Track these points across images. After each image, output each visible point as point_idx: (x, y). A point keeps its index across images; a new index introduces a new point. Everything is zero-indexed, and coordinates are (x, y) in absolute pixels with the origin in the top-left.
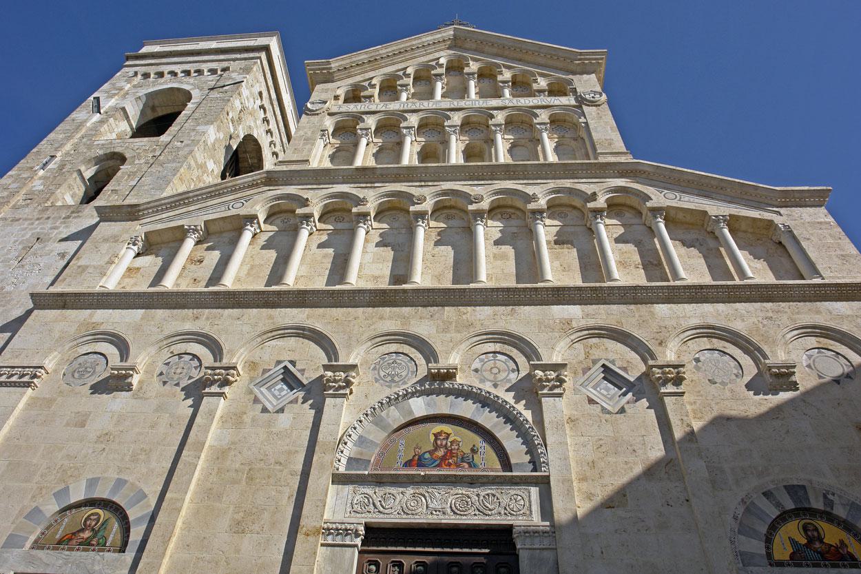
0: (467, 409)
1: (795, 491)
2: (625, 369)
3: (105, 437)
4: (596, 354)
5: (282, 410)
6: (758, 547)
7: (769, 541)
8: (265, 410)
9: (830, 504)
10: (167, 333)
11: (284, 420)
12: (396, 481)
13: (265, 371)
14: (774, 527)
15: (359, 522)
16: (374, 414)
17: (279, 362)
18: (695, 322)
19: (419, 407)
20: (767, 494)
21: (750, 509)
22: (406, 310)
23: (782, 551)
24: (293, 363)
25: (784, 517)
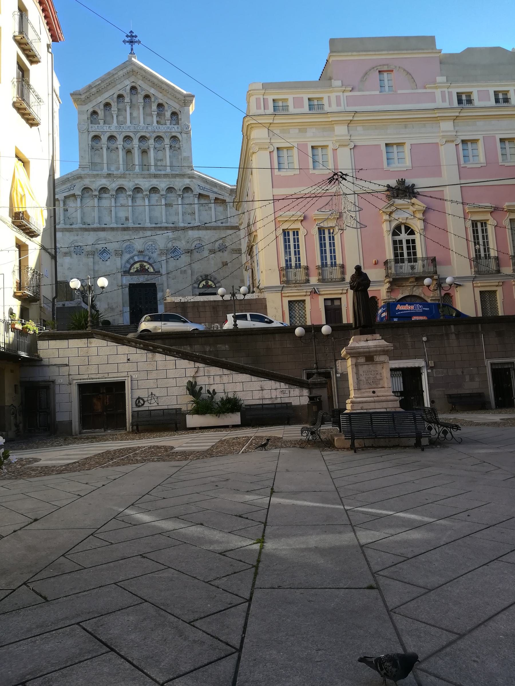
0: (146, 259)
1: (206, 276)
2: (180, 249)
3: (69, 269)
4: (174, 245)
5: (107, 260)
6: (196, 285)
7: (199, 284)
8: (103, 261)
9: (211, 278)
10: (71, 240)
11: (108, 263)
12: (133, 275)
13: (100, 250)
14: (201, 282)
15: (128, 284)
16: (128, 261)
17: (103, 248)
18: (197, 236)
19: (136, 259)
20: (201, 276)
21: (197, 279)
22: (130, 232)
23: (201, 286)
24: (106, 248)
25: (203, 280)
